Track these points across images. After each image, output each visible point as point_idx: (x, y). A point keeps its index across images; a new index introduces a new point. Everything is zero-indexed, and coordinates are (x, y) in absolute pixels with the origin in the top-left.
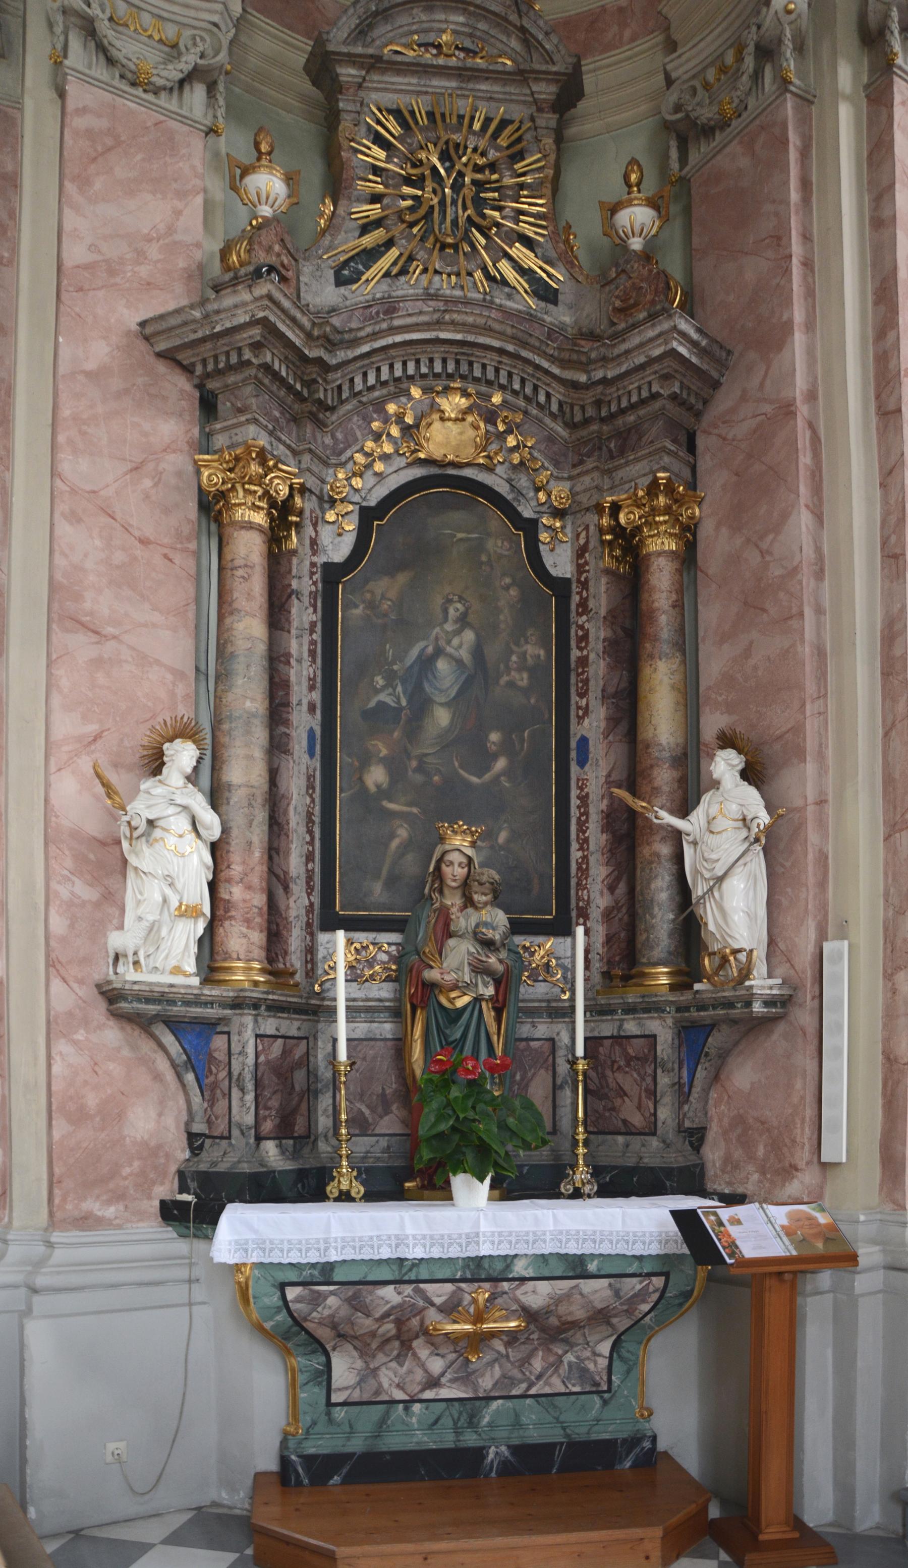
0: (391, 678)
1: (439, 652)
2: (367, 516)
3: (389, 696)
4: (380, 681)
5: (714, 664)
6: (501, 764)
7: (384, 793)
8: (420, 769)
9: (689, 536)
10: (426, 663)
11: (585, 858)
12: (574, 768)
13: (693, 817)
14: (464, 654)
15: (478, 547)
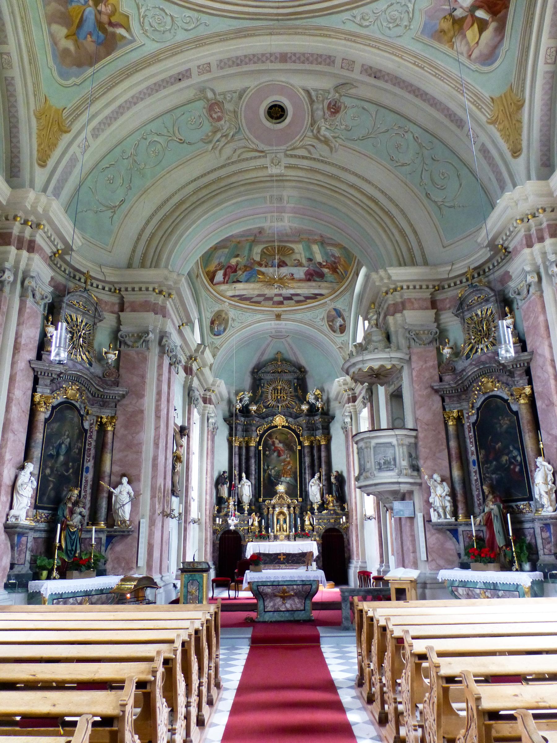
0: (53, 447)
1: (63, 443)
2: (53, 408)
3: (54, 452)
4: (51, 448)
5: (117, 456)
6: (71, 471)
7: (50, 476)
8: (56, 470)
9: (114, 427)
10: (60, 445)
11: (86, 495)
12: (84, 473)
13: (116, 489)
14: (67, 444)
15: (72, 419)
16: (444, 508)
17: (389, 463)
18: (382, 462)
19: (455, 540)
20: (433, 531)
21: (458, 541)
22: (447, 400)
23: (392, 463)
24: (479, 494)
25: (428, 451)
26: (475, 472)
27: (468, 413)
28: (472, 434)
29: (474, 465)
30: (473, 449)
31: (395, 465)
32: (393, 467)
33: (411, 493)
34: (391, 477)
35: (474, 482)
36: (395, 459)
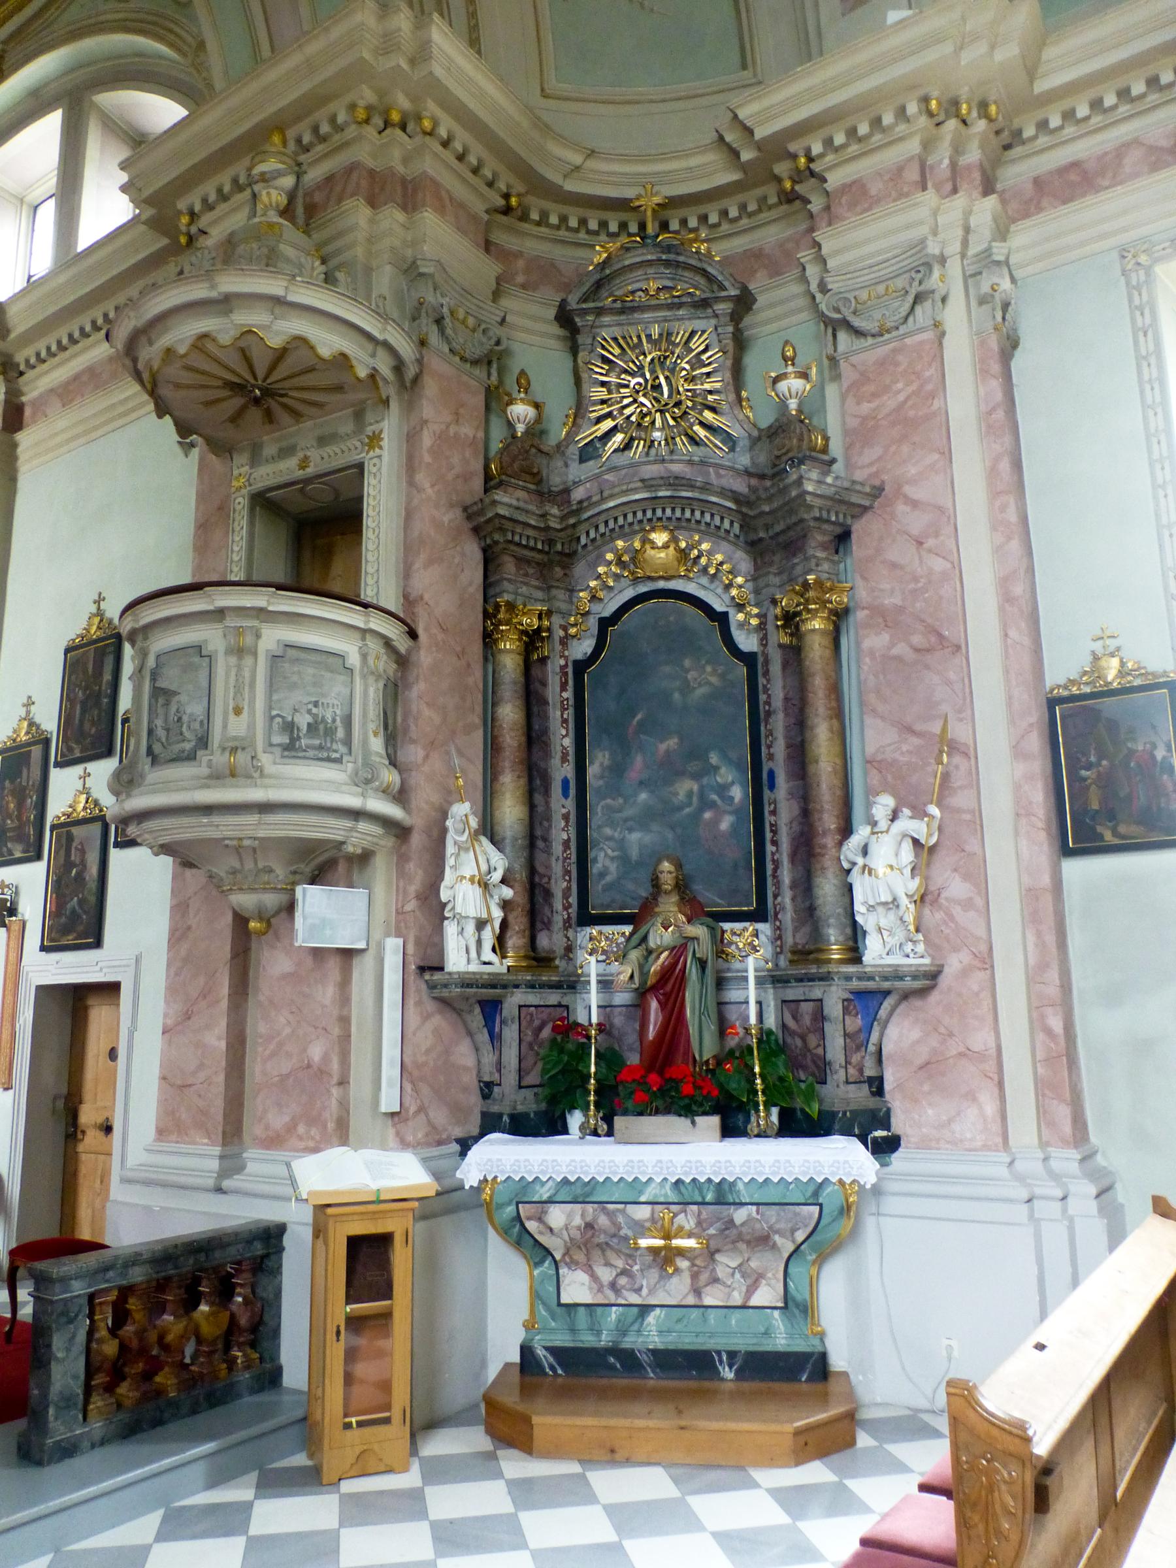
16: (481, 924)
17: (330, 732)
18: (303, 721)
19: (484, 1036)
20: (430, 1006)
21: (495, 1038)
22: (509, 567)
23: (340, 733)
24: (569, 888)
25: (437, 720)
26: (566, 817)
27: (565, 628)
28: (568, 694)
29: (566, 794)
30: (568, 742)
31: (348, 742)
32: (343, 749)
33: (364, 858)
34: (336, 787)
35: (557, 849)
36: (348, 721)
